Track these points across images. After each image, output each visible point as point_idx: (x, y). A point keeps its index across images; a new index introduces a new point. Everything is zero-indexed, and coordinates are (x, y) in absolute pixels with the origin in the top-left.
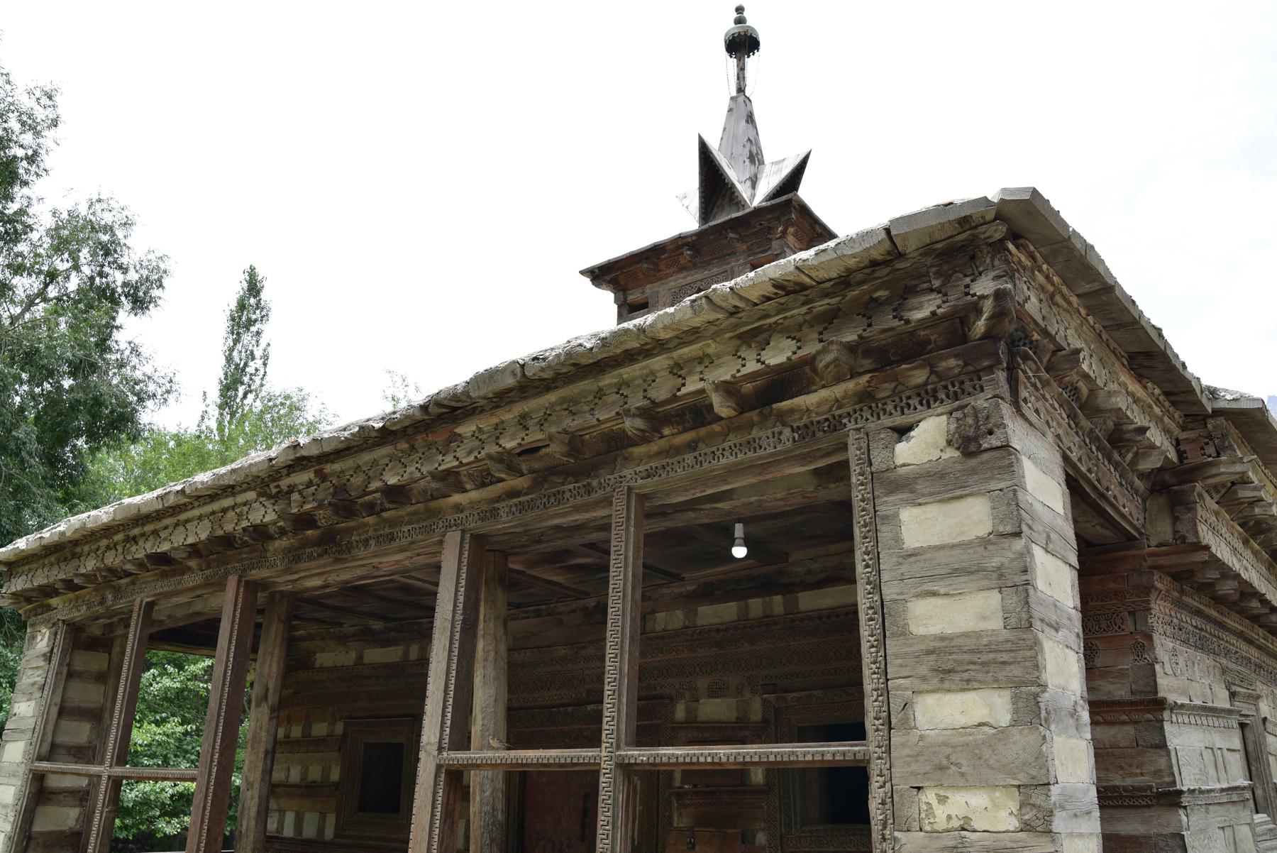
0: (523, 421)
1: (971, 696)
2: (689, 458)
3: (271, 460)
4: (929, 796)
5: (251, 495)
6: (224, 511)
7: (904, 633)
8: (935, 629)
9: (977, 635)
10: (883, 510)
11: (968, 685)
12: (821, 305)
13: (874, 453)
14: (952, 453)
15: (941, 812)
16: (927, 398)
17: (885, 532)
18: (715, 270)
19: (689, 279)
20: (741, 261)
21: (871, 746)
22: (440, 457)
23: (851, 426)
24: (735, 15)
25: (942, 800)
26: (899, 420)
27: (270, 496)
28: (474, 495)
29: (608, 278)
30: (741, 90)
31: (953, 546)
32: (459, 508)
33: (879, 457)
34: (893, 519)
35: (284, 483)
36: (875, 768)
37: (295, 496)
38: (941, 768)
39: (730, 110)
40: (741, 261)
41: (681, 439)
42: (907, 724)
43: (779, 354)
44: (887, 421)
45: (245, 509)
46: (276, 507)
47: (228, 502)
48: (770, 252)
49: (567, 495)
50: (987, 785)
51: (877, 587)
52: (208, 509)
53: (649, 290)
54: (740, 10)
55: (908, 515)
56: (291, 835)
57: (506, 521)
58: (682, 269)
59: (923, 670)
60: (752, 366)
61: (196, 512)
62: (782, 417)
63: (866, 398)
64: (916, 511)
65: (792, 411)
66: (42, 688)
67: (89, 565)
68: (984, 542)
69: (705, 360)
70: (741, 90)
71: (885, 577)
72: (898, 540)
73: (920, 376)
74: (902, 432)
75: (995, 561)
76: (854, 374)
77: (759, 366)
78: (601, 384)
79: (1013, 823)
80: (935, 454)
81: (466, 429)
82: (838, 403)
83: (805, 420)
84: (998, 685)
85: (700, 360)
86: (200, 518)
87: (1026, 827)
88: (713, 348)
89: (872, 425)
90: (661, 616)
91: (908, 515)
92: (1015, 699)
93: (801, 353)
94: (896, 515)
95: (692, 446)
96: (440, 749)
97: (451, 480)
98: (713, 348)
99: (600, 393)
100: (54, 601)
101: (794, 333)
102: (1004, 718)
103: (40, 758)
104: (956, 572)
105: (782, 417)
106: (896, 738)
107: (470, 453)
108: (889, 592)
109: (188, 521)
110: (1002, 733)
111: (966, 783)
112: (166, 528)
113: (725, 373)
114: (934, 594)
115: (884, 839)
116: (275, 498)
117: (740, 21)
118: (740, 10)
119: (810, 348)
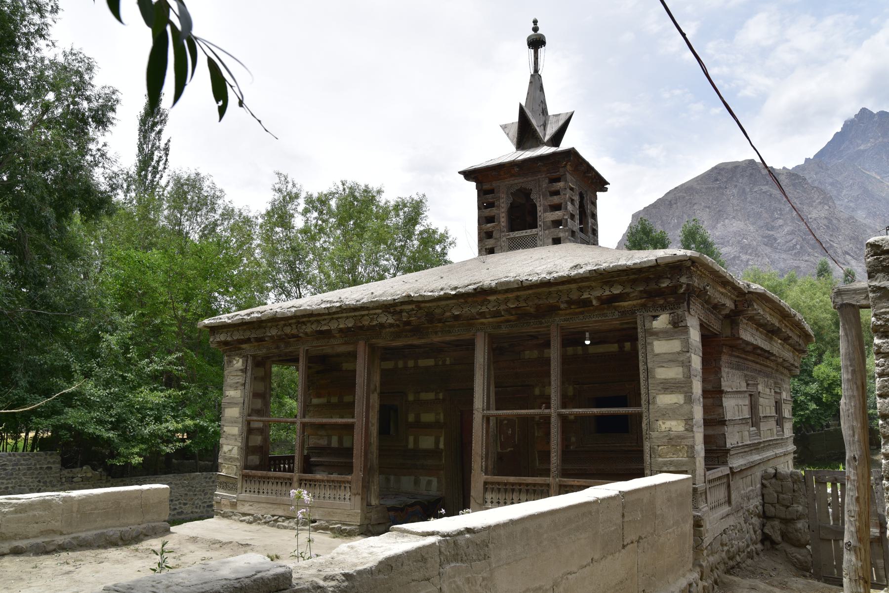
0: (517, 298)
1: (673, 396)
2: (581, 317)
3: (394, 300)
4: (660, 422)
5: (380, 311)
6: (363, 316)
7: (654, 377)
8: (663, 377)
9: (675, 379)
10: (648, 341)
11: (672, 392)
12: (632, 277)
13: (646, 323)
14: (670, 326)
15: (663, 427)
16: (663, 308)
17: (649, 348)
18: (530, 179)
19: (516, 181)
20: (543, 176)
21: (644, 408)
22: (480, 307)
23: (638, 313)
24: (532, 25)
25: (664, 423)
26: (654, 314)
27: (390, 313)
28: (491, 320)
29: (473, 176)
30: (536, 71)
31: (670, 353)
32: (482, 324)
33: (647, 325)
34: (651, 344)
35: (398, 309)
36: (644, 415)
37: (404, 314)
38: (664, 415)
39: (531, 82)
40: (543, 176)
41: (577, 310)
42: (654, 403)
43: (617, 290)
44: (650, 314)
45: (375, 316)
46: (394, 318)
47: (366, 312)
48: (558, 173)
49: (532, 324)
50: (677, 419)
51: (646, 363)
52: (353, 314)
53: (495, 184)
54: (535, 22)
55: (656, 343)
56: (337, 446)
57: (504, 330)
58: (512, 176)
59: (659, 388)
60: (607, 293)
61: (345, 315)
62: (615, 308)
63: (644, 306)
64: (659, 342)
65: (618, 306)
66: (244, 385)
67: (274, 332)
68: (678, 353)
69: (591, 288)
70: (536, 71)
71: (648, 361)
72: (653, 350)
73: (661, 302)
74: (655, 317)
75: (681, 359)
76: (641, 298)
77: (610, 293)
78: (550, 290)
79: (683, 429)
80: (665, 327)
81: (492, 298)
82: (634, 306)
83: (623, 310)
84: (680, 392)
85: (588, 287)
86: (347, 318)
87: (686, 430)
88: (593, 284)
89: (646, 314)
90: (527, 352)
91: (656, 343)
92: (685, 396)
93: (624, 291)
94: (652, 343)
95: (582, 313)
96: (483, 410)
97: (482, 315)
98: (593, 284)
99: (550, 293)
100: (244, 346)
101: (622, 284)
102: (682, 402)
103: (249, 415)
105: (615, 308)
106: (651, 407)
107: (494, 307)
108: (650, 365)
109: (339, 318)
110: (681, 405)
111: (670, 419)
112: (325, 319)
113: (598, 293)
114: (663, 367)
115: (647, 434)
116: (393, 314)
117: (535, 29)
118: (535, 22)
119: (628, 290)
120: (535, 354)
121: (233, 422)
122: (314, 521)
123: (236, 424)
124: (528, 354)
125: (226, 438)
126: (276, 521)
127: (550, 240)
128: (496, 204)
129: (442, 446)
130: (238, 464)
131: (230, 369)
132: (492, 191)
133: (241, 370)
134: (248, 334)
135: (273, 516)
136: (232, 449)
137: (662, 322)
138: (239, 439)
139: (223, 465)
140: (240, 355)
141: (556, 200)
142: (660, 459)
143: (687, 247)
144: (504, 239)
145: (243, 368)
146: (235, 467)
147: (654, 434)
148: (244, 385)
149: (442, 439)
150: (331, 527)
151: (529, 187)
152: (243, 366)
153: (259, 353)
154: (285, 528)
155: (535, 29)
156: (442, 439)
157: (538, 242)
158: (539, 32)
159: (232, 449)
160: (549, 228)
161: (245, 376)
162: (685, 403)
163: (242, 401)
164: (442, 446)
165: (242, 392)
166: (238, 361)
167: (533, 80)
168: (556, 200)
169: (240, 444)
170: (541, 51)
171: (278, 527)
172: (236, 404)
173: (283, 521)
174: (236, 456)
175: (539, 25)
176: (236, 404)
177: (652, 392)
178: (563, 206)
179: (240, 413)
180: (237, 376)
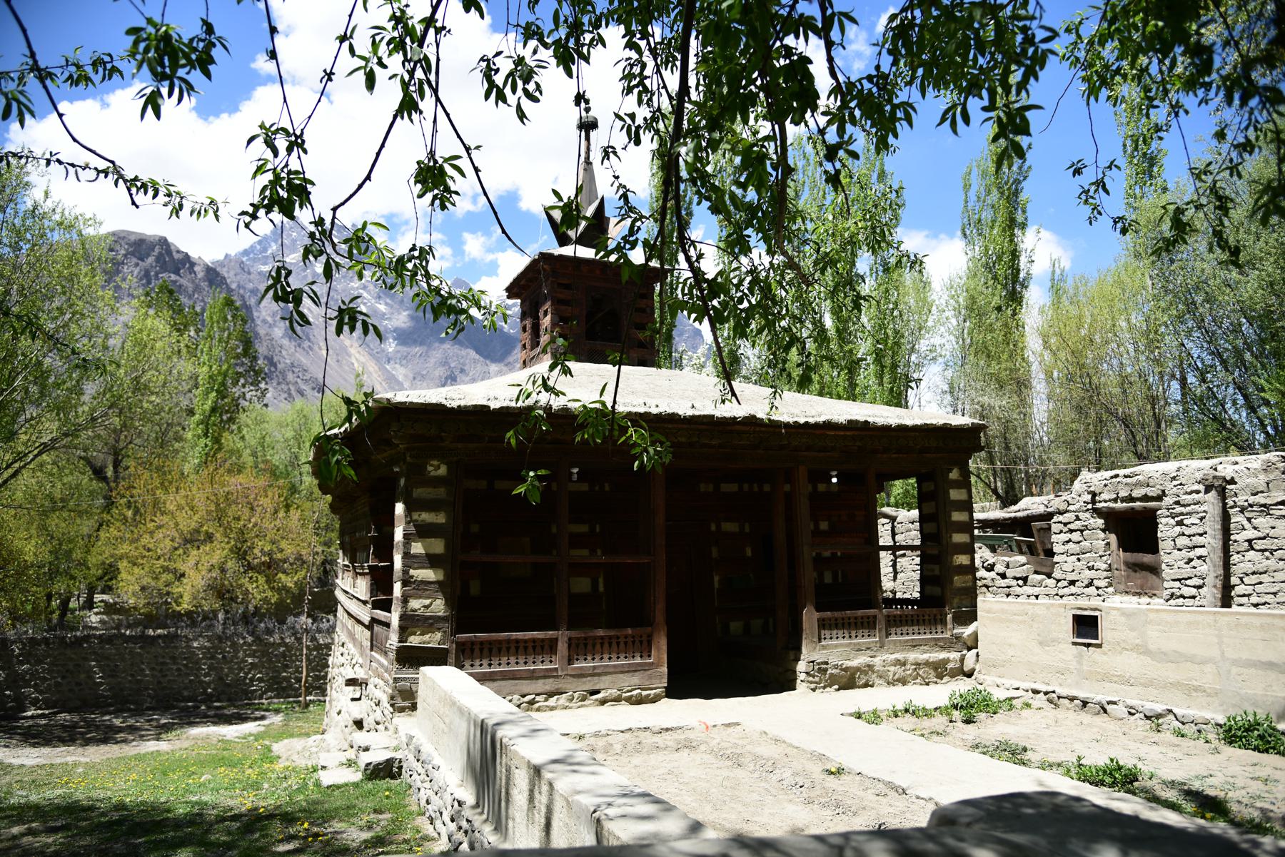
74: (951, 471)
120: (711, 488)
122: (597, 692)
124: (703, 487)
126: (532, 703)
129: (601, 589)
135: (524, 696)
136: (431, 603)
143: (975, 418)
149: (601, 580)
150: (624, 695)
154: (552, 709)
156: (601, 580)
158: (591, 113)
159: (431, 603)
164: (601, 589)
166: (439, 468)
170: (593, 134)
171: (538, 710)
173: (546, 700)
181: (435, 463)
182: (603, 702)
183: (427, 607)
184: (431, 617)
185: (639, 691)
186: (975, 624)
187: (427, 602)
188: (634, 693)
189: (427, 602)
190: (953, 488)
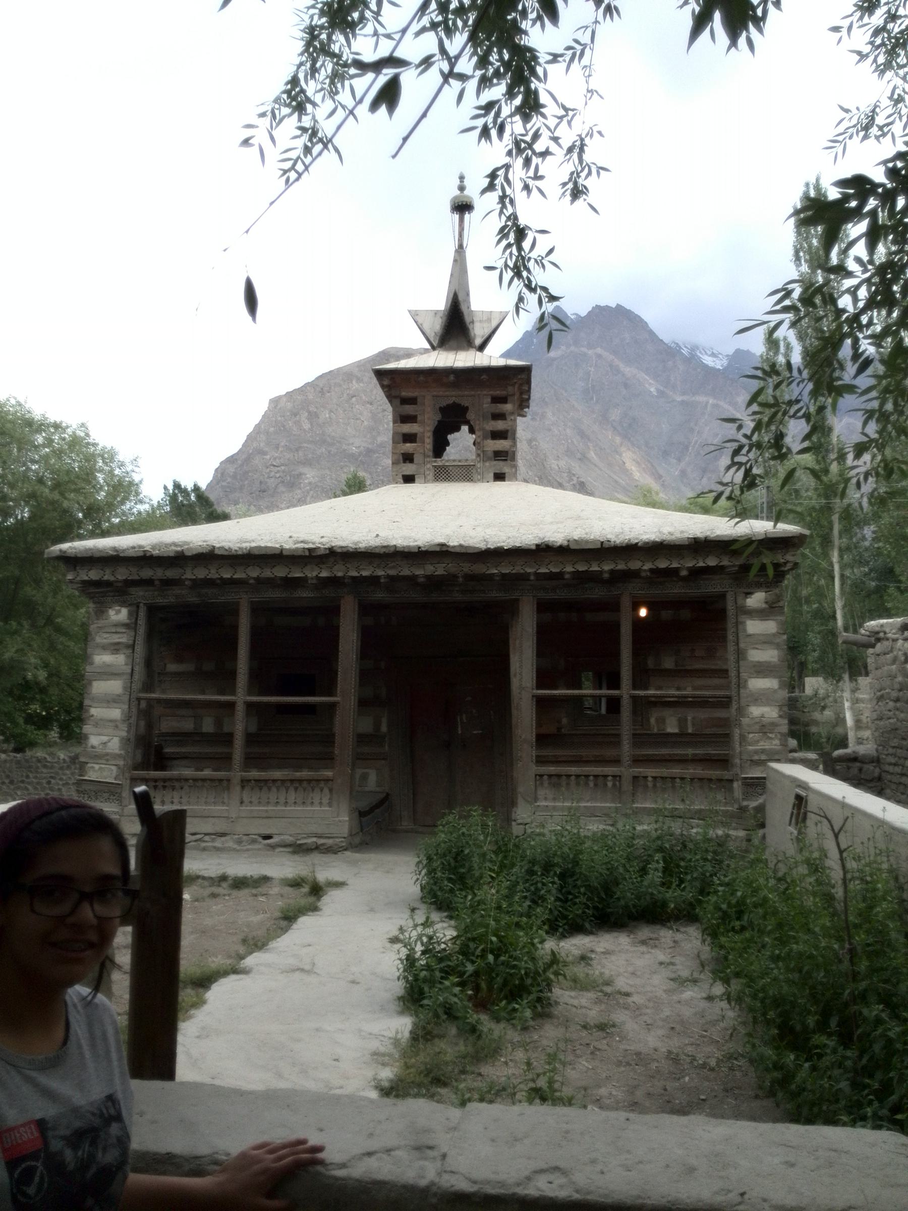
1: (766, 680)
8: (756, 659)
9: (770, 662)
10: (742, 618)
17: (740, 627)
24: (458, 182)
26: (749, 591)
33: (740, 601)
34: (744, 623)
42: (745, 687)
51: (737, 644)
54: (462, 178)
64: (752, 622)
68: (774, 635)
70: (461, 246)
72: (745, 630)
84: (775, 677)
93: (721, 564)
100: (133, 590)
104: (765, 643)
106: (742, 691)
108: (742, 645)
110: (775, 691)
117: (462, 188)
118: (462, 178)
121: (110, 701)
122: (268, 837)
123: (115, 705)
125: (96, 725)
127: (492, 475)
128: (419, 418)
130: (121, 763)
131: (101, 623)
132: (412, 401)
133: (126, 625)
134: (147, 573)
137: (757, 599)
138: (124, 727)
139: (89, 765)
140: (123, 604)
141: (500, 425)
142: (751, 748)
144: (429, 466)
145: (128, 621)
146: (114, 768)
147: (745, 721)
148: (132, 647)
150: (299, 842)
151: (465, 403)
152: (129, 618)
153: (160, 601)
155: (462, 188)
157: (476, 476)
158: (466, 192)
160: (489, 459)
161: (133, 633)
162: (780, 688)
163: (129, 671)
164: (384, 728)
165: (127, 657)
166: (118, 612)
167: (458, 258)
168: (500, 425)
169: (124, 734)
172: (116, 674)
173: (213, 840)
174: (117, 751)
175: (466, 182)
176: (116, 674)
177: (744, 675)
178: (509, 434)
179: (125, 688)
180: (116, 633)
181: (117, 608)
182: (273, 847)
183: (105, 744)
184: (107, 754)
185: (314, 839)
186: (764, 797)
187: (105, 739)
188: (309, 841)
189: (105, 739)
190: (752, 618)
